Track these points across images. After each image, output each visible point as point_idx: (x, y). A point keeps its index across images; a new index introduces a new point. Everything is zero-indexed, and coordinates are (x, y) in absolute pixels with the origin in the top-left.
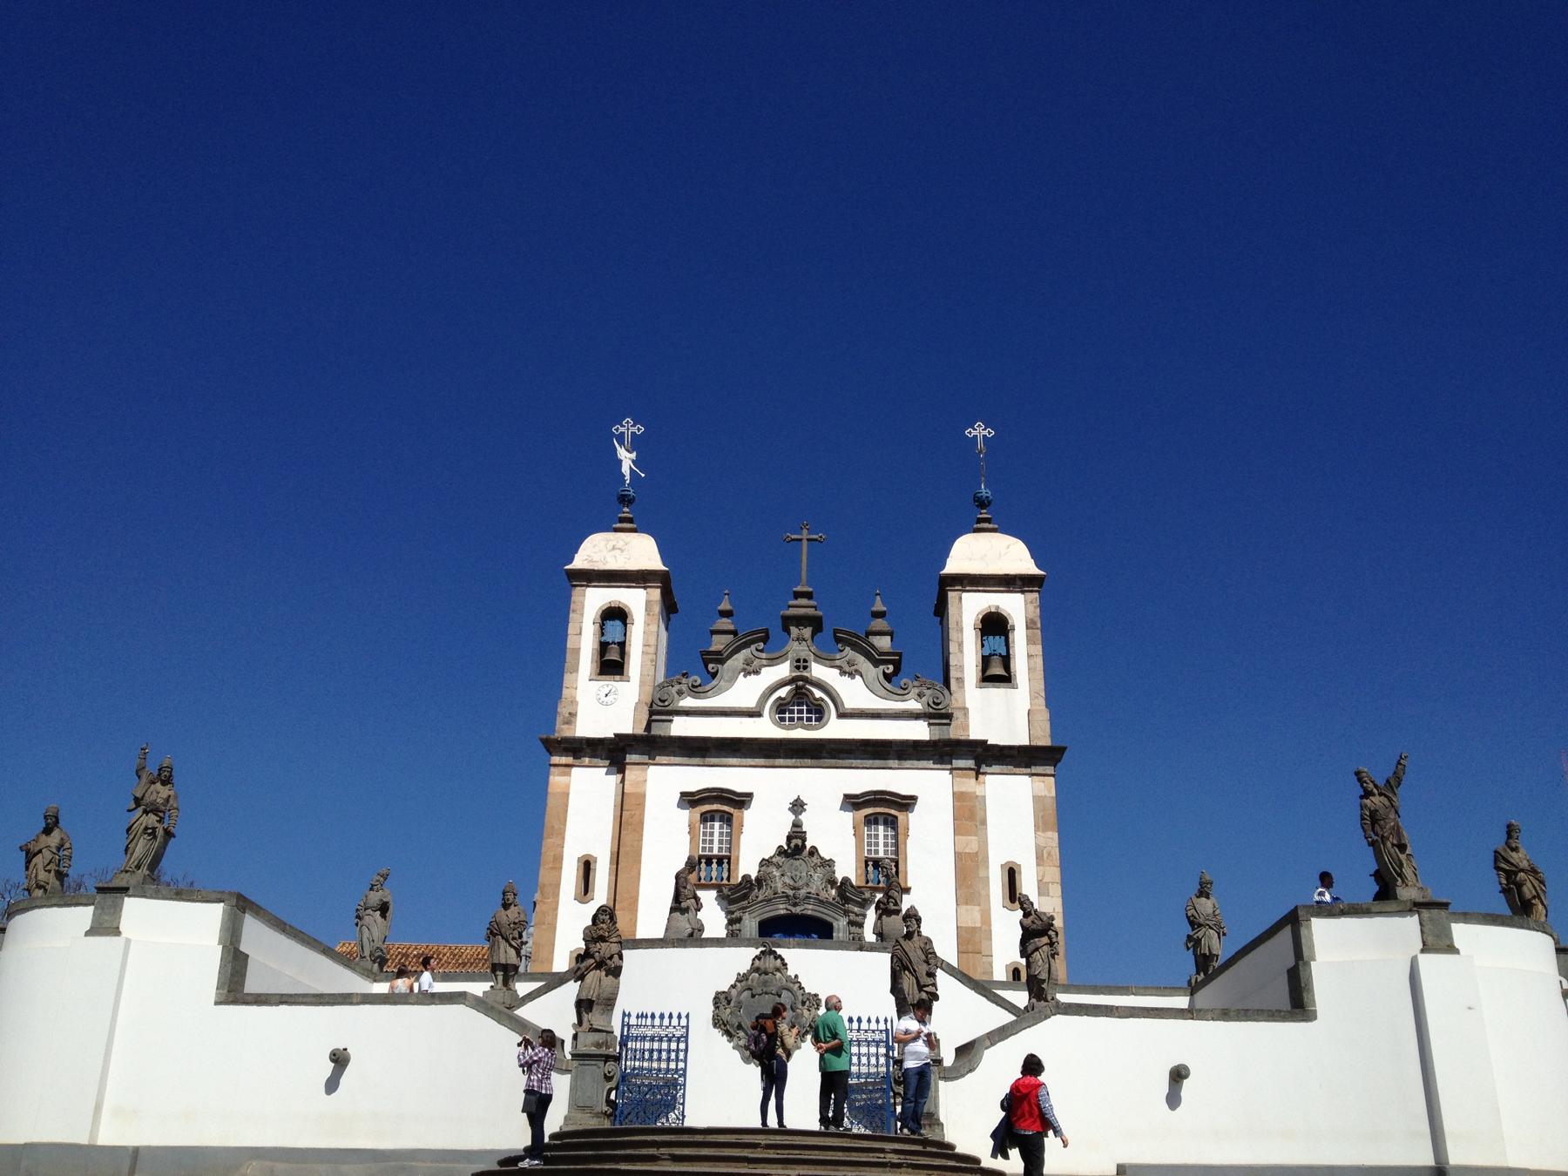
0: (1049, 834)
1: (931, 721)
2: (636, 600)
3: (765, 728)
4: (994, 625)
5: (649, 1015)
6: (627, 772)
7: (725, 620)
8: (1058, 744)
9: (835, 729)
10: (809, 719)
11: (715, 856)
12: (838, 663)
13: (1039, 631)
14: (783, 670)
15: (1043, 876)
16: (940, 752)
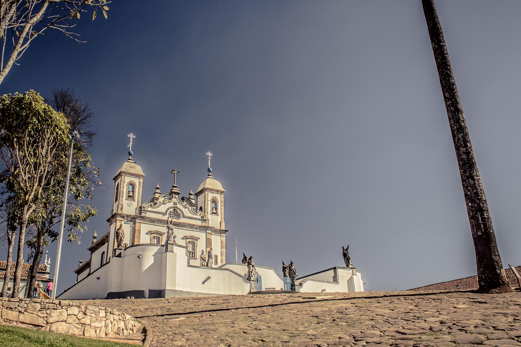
1: (203, 221)
2: (136, 181)
4: (214, 201)
7: (158, 190)
8: (226, 230)
9: (182, 220)
10: (176, 217)
12: (183, 205)
13: (223, 204)
16: (205, 228)
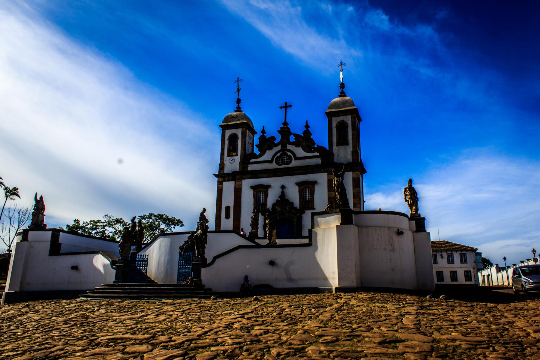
0: (357, 189)
3: (274, 166)
4: (342, 126)
5: (140, 255)
6: (236, 182)
11: (261, 204)
14: (279, 148)
15: (355, 202)
